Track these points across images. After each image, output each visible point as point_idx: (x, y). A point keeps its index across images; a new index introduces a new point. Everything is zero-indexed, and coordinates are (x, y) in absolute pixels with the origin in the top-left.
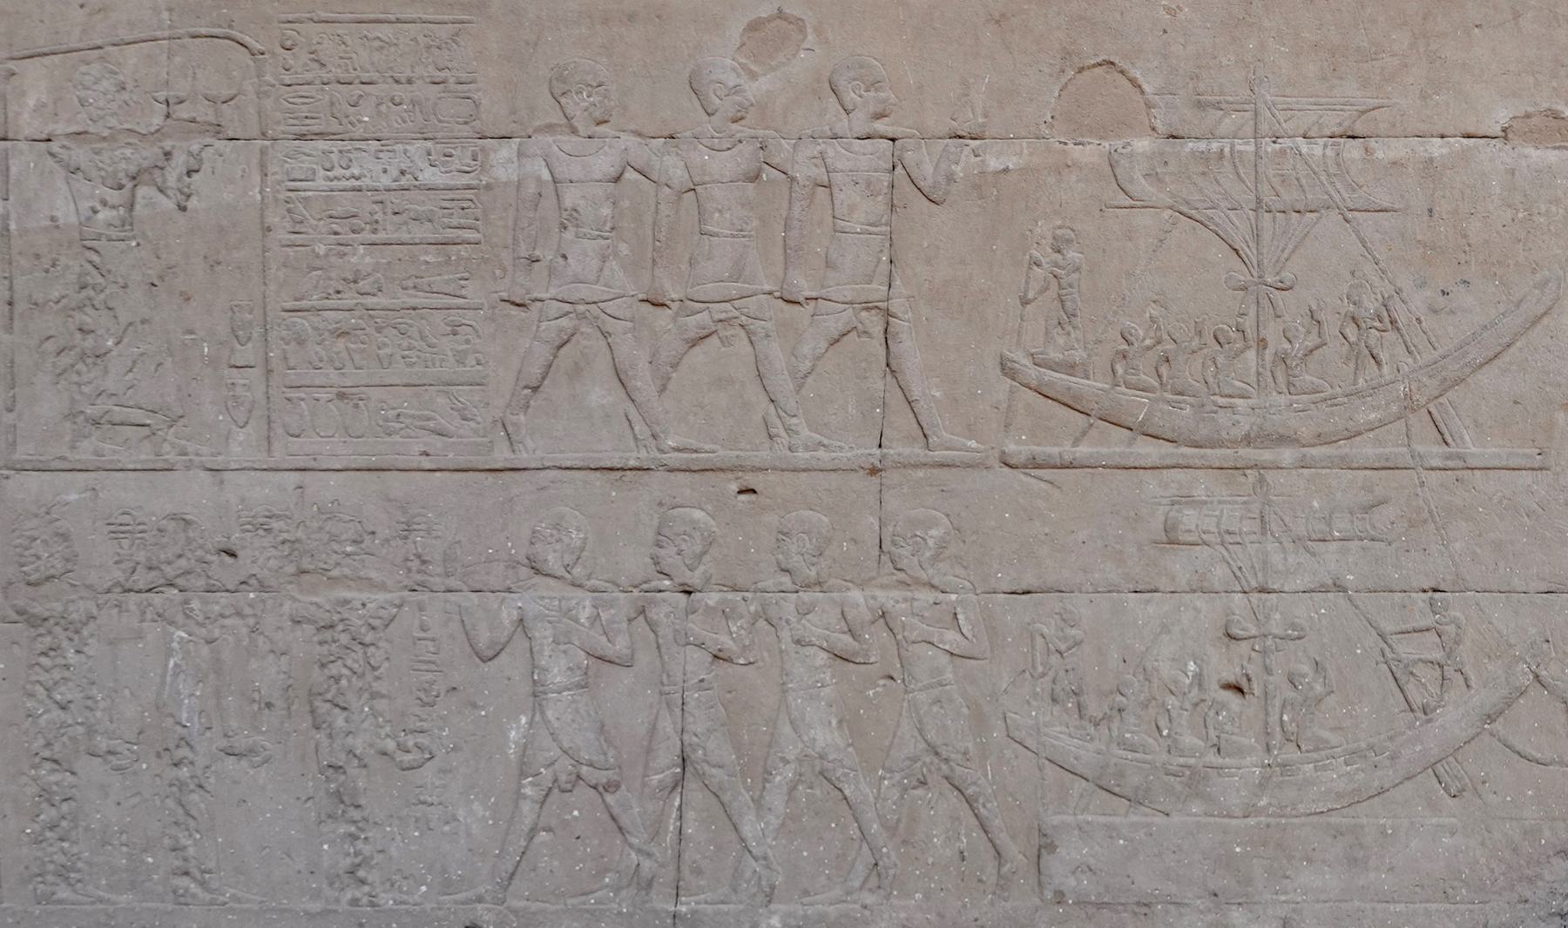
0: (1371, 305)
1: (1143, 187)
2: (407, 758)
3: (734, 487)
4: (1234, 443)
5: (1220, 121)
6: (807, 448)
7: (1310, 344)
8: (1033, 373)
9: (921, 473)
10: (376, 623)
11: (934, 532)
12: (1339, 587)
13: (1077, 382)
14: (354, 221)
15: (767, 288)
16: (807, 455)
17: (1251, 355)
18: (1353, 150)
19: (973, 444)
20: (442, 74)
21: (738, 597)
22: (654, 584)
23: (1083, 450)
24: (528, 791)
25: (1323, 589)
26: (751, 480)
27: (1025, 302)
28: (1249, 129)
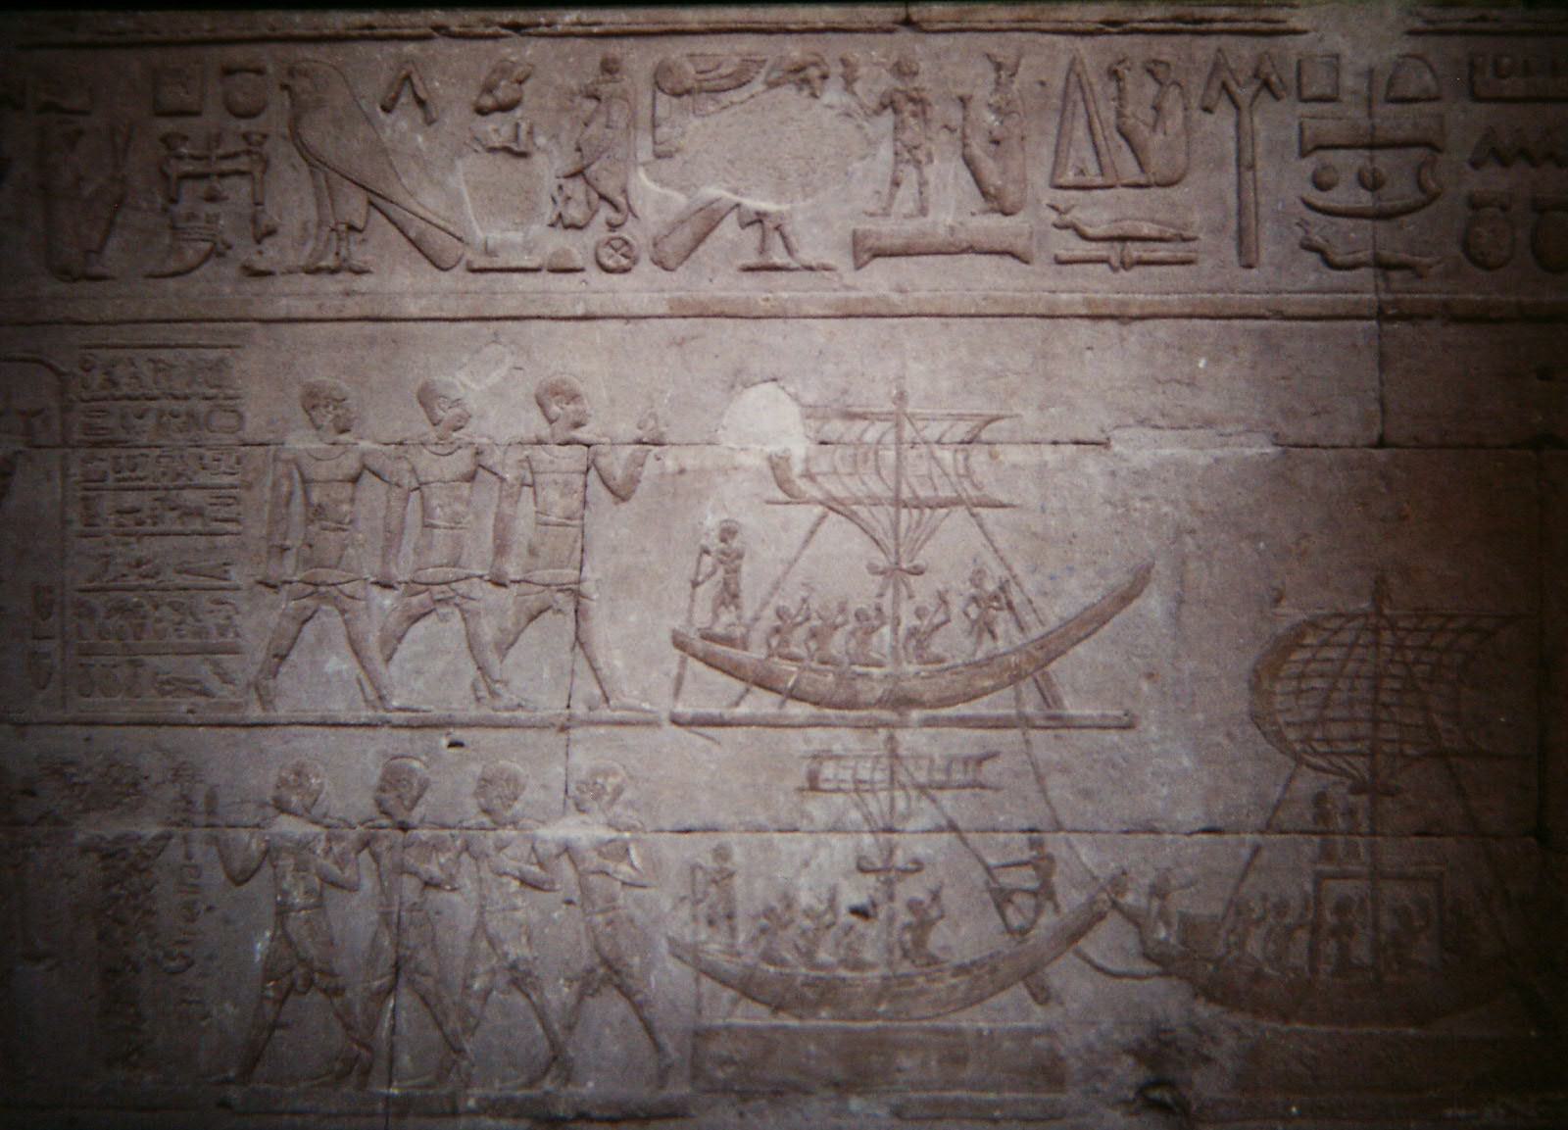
0: (991, 587)
1: (803, 485)
2: (172, 964)
3: (444, 742)
4: (867, 706)
5: (865, 431)
6: (507, 709)
7: (936, 620)
8: (699, 645)
9: (602, 730)
10: (149, 852)
11: (611, 780)
12: (953, 827)
13: (736, 653)
14: (138, 515)
15: (480, 573)
16: (506, 715)
17: (886, 630)
18: (979, 457)
19: (646, 706)
20: (214, 391)
21: (446, 833)
22: (377, 823)
23: (743, 710)
24: (271, 993)
25: (939, 830)
26: (458, 734)
27: (695, 584)
28: (890, 438)
